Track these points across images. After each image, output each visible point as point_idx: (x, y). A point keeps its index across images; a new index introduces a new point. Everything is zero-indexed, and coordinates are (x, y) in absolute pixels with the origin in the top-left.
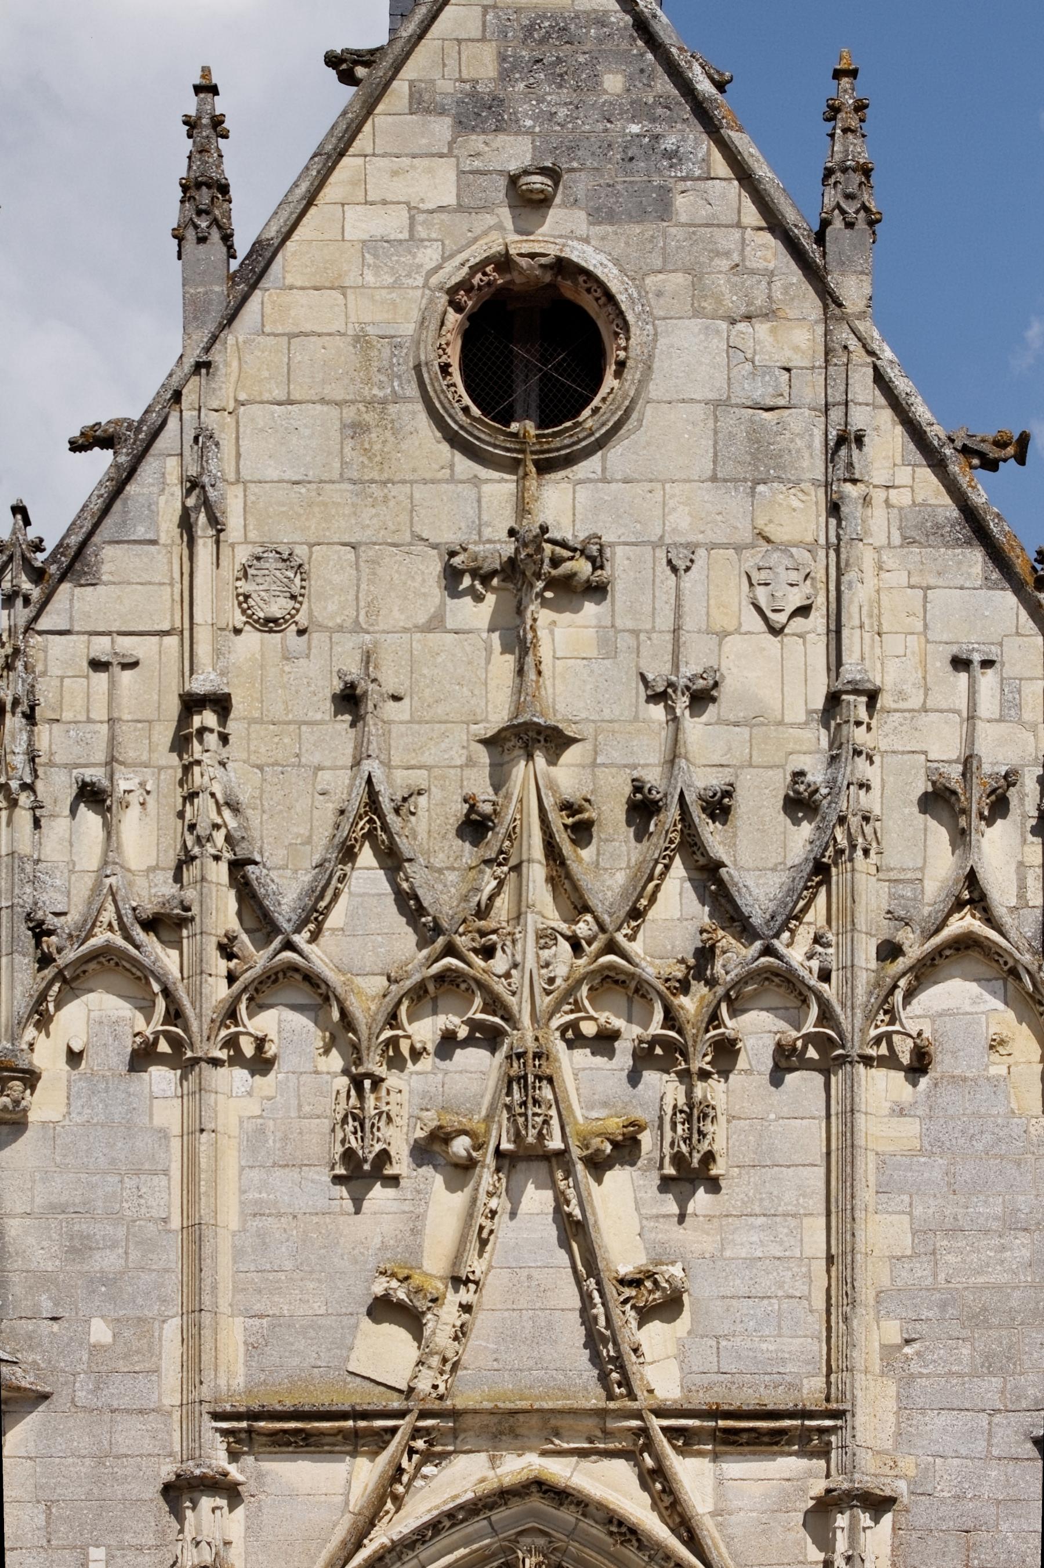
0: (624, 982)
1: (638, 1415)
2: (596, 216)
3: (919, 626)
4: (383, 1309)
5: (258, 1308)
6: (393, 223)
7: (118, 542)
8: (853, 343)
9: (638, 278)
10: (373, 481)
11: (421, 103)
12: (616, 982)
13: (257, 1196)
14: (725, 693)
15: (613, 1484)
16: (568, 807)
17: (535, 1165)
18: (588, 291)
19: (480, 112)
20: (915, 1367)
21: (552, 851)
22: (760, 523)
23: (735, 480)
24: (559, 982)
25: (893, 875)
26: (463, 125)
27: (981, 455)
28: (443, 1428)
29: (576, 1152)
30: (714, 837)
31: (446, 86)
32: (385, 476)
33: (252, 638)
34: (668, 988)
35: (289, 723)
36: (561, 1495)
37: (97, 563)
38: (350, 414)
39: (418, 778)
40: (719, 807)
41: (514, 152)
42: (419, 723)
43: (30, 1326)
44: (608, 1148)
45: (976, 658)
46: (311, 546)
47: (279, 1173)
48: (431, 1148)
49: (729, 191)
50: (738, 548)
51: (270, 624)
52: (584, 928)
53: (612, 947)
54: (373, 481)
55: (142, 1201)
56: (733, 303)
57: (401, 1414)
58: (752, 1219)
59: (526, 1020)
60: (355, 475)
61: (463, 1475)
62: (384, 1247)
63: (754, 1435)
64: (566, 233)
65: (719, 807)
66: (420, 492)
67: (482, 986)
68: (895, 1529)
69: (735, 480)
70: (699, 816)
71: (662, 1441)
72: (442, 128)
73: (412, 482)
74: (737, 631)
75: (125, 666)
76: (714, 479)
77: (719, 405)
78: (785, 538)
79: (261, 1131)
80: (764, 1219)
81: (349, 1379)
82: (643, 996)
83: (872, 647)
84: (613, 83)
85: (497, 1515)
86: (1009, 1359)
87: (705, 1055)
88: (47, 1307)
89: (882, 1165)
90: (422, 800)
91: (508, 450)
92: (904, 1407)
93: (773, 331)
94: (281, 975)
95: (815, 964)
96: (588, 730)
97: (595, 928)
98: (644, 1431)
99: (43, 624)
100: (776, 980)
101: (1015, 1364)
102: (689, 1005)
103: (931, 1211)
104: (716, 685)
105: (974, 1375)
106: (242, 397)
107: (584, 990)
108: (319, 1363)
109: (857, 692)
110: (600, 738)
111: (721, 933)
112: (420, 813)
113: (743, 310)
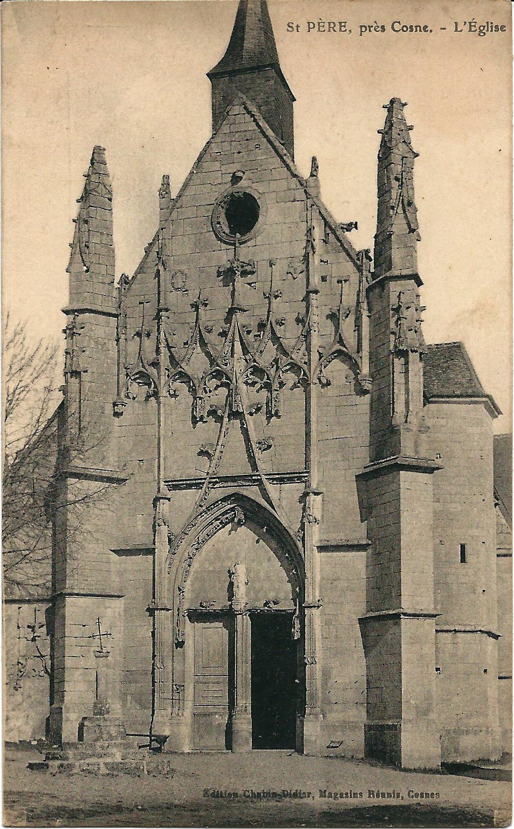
4: (201, 453)
15: (252, 492)
41: (232, 168)
48: (212, 413)
53: (255, 361)
61: (217, 493)
102: (272, 371)
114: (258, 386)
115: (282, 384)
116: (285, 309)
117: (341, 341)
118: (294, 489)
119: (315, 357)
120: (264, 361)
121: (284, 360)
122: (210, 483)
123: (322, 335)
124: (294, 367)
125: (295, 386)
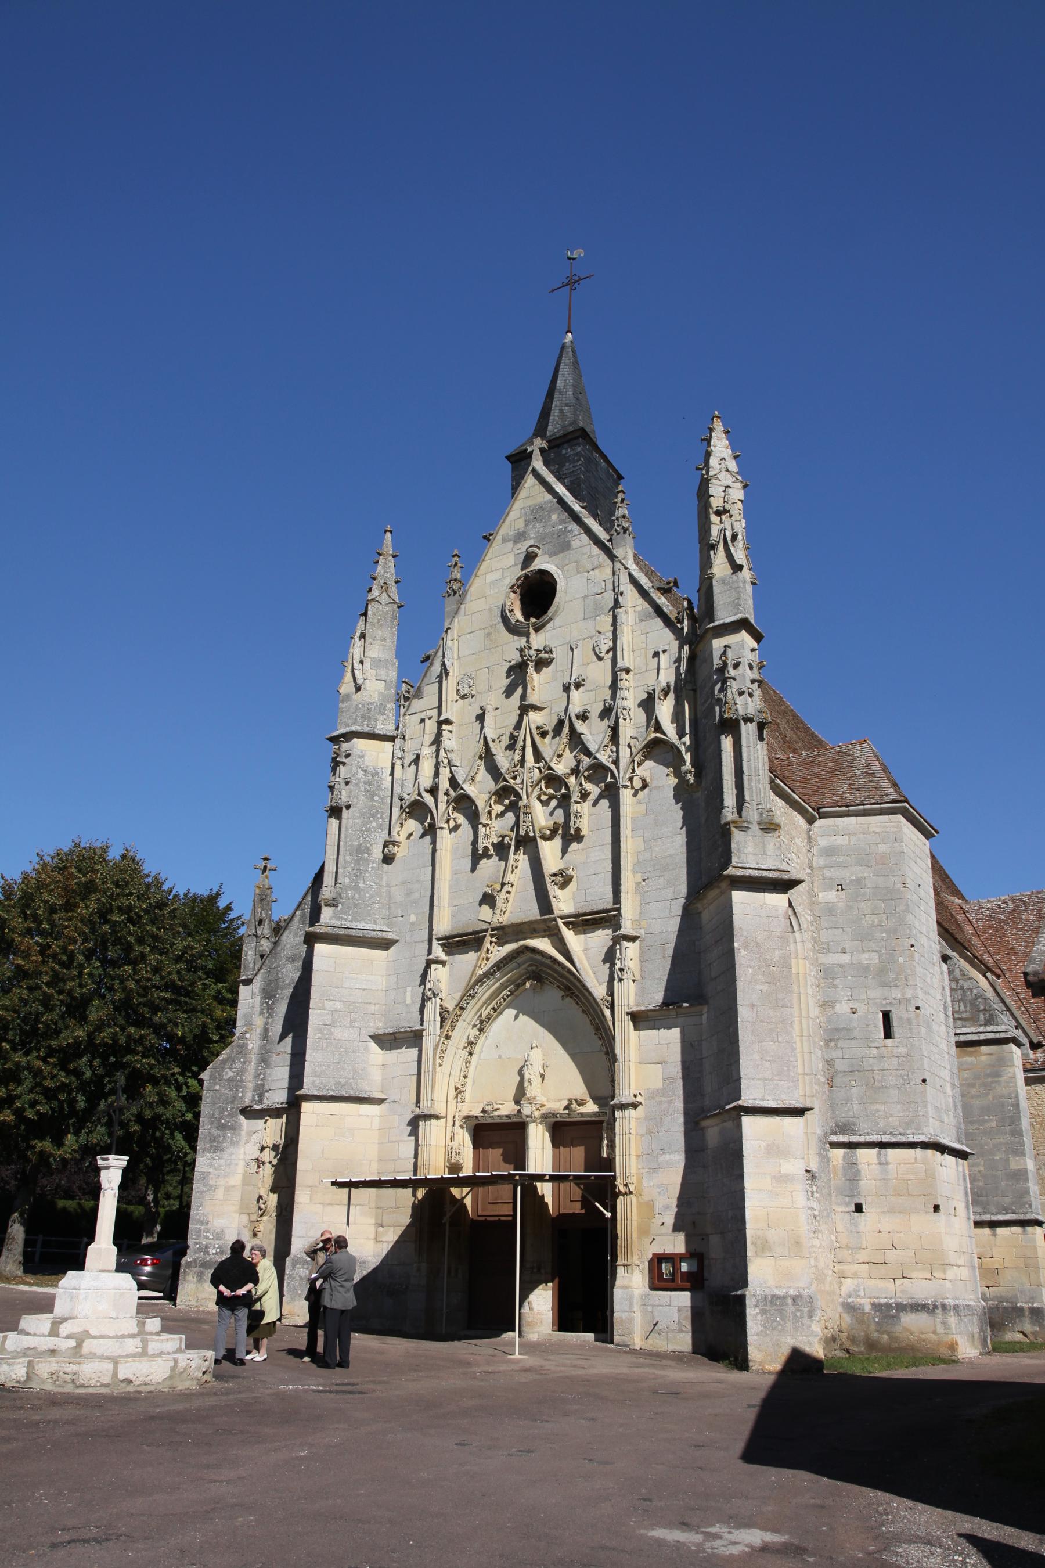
1: (555, 919)
2: (551, 555)
3: (644, 645)
5: (455, 903)
6: (497, 575)
8: (622, 567)
9: (562, 569)
11: (505, 540)
16: (538, 728)
19: (520, 537)
20: (646, 889)
26: (515, 542)
27: (663, 589)
28: (504, 933)
30: (580, 727)
31: (511, 533)
33: (461, 701)
36: (534, 950)
38: (487, 631)
39: (502, 731)
40: (583, 717)
44: (548, 832)
45: (660, 650)
49: (584, 537)
50: (591, 638)
51: (463, 697)
52: (541, 765)
53: (550, 768)
56: (589, 567)
64: (541, 563)
68: (641, 947)
70: (574, 719)
72: (510, 544)
84: (554, 517)
85: (519, 960)
96: (549, 704)
98: (557, 925)
102: (572, 780)
107: (543, 782)
109: (621, 670)
114: (554, 803)
117: (658, 728)
118: (602, 937)
119: (625, 753)
120: (561, 768)
121: (586, 761)
122: (492, 936)
125: (601, 797)
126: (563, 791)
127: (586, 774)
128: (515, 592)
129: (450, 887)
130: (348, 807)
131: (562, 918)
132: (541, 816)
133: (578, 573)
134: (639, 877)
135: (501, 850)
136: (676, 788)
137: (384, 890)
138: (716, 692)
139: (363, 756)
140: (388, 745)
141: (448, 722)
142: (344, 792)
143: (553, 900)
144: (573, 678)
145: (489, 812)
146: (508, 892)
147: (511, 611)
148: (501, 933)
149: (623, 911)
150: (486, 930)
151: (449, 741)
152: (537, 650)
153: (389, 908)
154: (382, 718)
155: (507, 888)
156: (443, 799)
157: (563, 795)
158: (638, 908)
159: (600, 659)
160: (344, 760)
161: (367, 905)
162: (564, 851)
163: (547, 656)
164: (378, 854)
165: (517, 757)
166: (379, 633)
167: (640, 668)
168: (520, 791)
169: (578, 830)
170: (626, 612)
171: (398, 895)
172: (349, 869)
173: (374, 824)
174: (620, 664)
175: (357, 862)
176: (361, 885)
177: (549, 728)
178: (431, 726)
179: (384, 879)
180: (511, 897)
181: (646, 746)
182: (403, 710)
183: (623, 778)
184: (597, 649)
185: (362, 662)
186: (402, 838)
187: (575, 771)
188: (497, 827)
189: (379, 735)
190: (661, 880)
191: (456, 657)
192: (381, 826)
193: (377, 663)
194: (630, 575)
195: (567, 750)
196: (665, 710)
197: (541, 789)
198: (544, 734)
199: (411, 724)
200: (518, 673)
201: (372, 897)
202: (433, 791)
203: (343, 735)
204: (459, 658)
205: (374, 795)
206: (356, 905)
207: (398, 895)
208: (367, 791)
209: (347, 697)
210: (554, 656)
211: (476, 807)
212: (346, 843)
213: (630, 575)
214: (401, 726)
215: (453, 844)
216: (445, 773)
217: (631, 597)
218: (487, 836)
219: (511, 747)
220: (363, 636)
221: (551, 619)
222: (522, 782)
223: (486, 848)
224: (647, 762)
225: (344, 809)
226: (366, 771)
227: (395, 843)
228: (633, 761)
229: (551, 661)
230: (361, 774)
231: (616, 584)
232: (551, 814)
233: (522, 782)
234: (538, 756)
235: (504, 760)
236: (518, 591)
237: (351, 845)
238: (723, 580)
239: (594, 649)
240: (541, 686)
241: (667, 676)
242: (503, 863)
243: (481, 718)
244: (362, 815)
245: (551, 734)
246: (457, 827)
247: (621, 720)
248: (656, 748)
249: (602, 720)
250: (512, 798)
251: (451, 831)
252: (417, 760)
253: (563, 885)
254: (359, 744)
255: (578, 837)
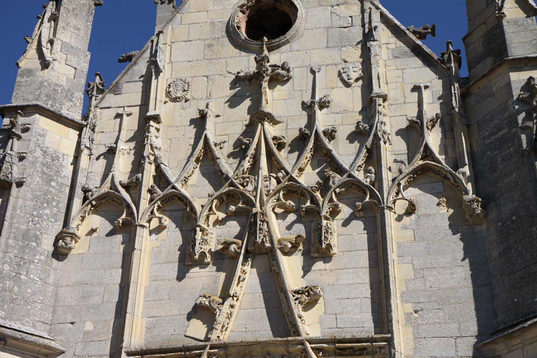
0: (296, 191)
1: (302, 343)
3: (401, 80)
5: (153, 314)
7: (129, 82)
8: (372, 7)
10: (214, 59)
12: (293, 192)
13: (156, 274)
14: (331, 104)
16: (275, 138)
17: (262, 256)
18: (285, 4)
21: (270, 154)
22: (344, 57)
23: (335, 47)
24: (271, 191)
25: (396, 153)
27: (419, 33)
29: (276, 246)
32: (218, 57)
33: (170, 104)
34: (312, 190)
35: (181, 126)
37: (122, 88)
38: (207, 42)
39: (225, 138)
40: (331, 135)
42: (226, 122)
43: (62, 326)
44: (290, 245)
45: (422, 85)
46: (192, 77)
47: (164, 265)
52: (280, 175)
53: (291, 179)
54: (214, 59)
55: (112, 278)
57: (204, 348)
58: (349, 270)
59: (258, 205)
60: (208, 58)
62: (203, 288)
63: (351, 350)
65: (331, 135)
66: (229, 60)
67: (243, 195)
69: (335, 47)
70: (322, 135)
71: (311, 351)
73: (227, 58)
74: (337, 87)
75: (128, 115)
76: (327, 47)
77: (328, 28)
78: (352, 61)
79: (160, 251)
80: (353, 270)
81: (186, 338)
82: (304, 196)
83: (384, 86)
86: (460, 316)
87: (327, 213)
88: (70, 319)
89: (399, 245)
90: (226, 144)
91: (258, 45)
92: (417, 338)
93: (346, 8)
94: (170, 198)
95: (368, 180)
97: (285, 174)
98: (305, 350)
99: (102, 105)
100: (353, 186)
101: (463, 318)
103: (421, 262)
104: (329, 102)
105: (446, 323)
106: (173, 41)
107: (281, 193)
108: (174, 333)
110: (289, 121)
111: (331, 172)
112: (224, 148)
113: (336, 3)
114: (292, 217)
115: (334, 212)
116: (343, 111)
117: (428, 153)
119: (387, 177)
121: (337, 179)
123: (394, 150)
124: (353, 187)
126: (308, 204)
127: (338, 190)
128: (244, 13)
129: (146, 295)
130: (20, 184)
131: (311, 341)
132: (279, 228)
133: (321, 5)
134: (409, 308)
135: (224, 259)
136: (450, 218)
137: (50, 289)
138: (520, 121)
139: (44, 136)
140: (73, 134)
141: (156, 119)
142: (15, 168)
143: (299, 320)
144: (317, 99)
145: (208, 217)
146: (232, 306)
147: (239, 28)
148: (222, 352)
149: (396, 341)
150: (204, 348)
151: (156, 137)
152: (275, 66)
153: (54, 312)
154: (68, 104)
155: (229, 301)
156: (145, 196)
157: (308, 211)
158: (412, 343)
159: (347, 85)
160: (19, 133)
161: (27, 302)
162: (306, 269)
163: (284, 72)
164: (48, 245)
165: (247, 164)
166: (73, 21)
167: (396, 99)
168: (253, 199)
169: (329, 246)
170: (380, 47)
171: (69, 297)
172: (11, 255)
173: (47, 211)
174: (376, 89)
175: (23, 249)
176: (22, 277)
177: (288, 140)
178: (131, 124)
179: (52, 277)
180: (235, 311)
181: (415, 172)
182: (94, 102)
183: (388, 197)
184: (344, 76)
185: (51, 42)
186: (81, 232)
187: (324, 186)
188: (216, 233)
189: (66, 118)
190: (441, 313)
191: (167, 60)
192: (55, 216)
193: (67, 48)
194: (382, 15)
195: (309, 166)
196: (433, 139)
197: (278, 200)
198: (280, 146)
199: (103, 118)
200: (248, 87)
201: (34, 294)
202: (133, 186)
203: (22, 108)
204: (171, 62)
205: (51, 180)
206: (13, 301)
207: (69, 297)
208: (43, 172)
209: (30, 72)
210: (291, 74)
211: (193, 209)
212: (11, 224)
213: (382, 15)
214: (91, 116)
215: (156, 245)
216: (150, 170)
217: (383, 34)
218: (204, 241)
219: (240, 150)
220: (54, 18)
221: (288, 42)
222: (256, 188)
223: (203, 254)
224: (410, 189)
225: (14, 186)
226: (45, 152)
227: (74, 236)
228: (399, 185)
229: (288, 80)
230: (38, 153)
231: (367, 20)
232: (289, 228)
233: (256, 188)
234: (274, 165)
235: (228, 166)
236: (247, 12)
237: (18, 228)
238: (516, 22)
239: (340, 74)
240: (274, 99)
241: (432, 109)
242: (222, 276)
243: (200, 122)
244: (35, 197)
245: (287, 148)
246: (160, 229)
247: (382, 142)
248: (425, 175)
249: (351, 142)
250: (240, 205)
251: (151, 232)
252: (111, 153)
253: (308, 306)
254: (40, 122)
255: (326, 255)
